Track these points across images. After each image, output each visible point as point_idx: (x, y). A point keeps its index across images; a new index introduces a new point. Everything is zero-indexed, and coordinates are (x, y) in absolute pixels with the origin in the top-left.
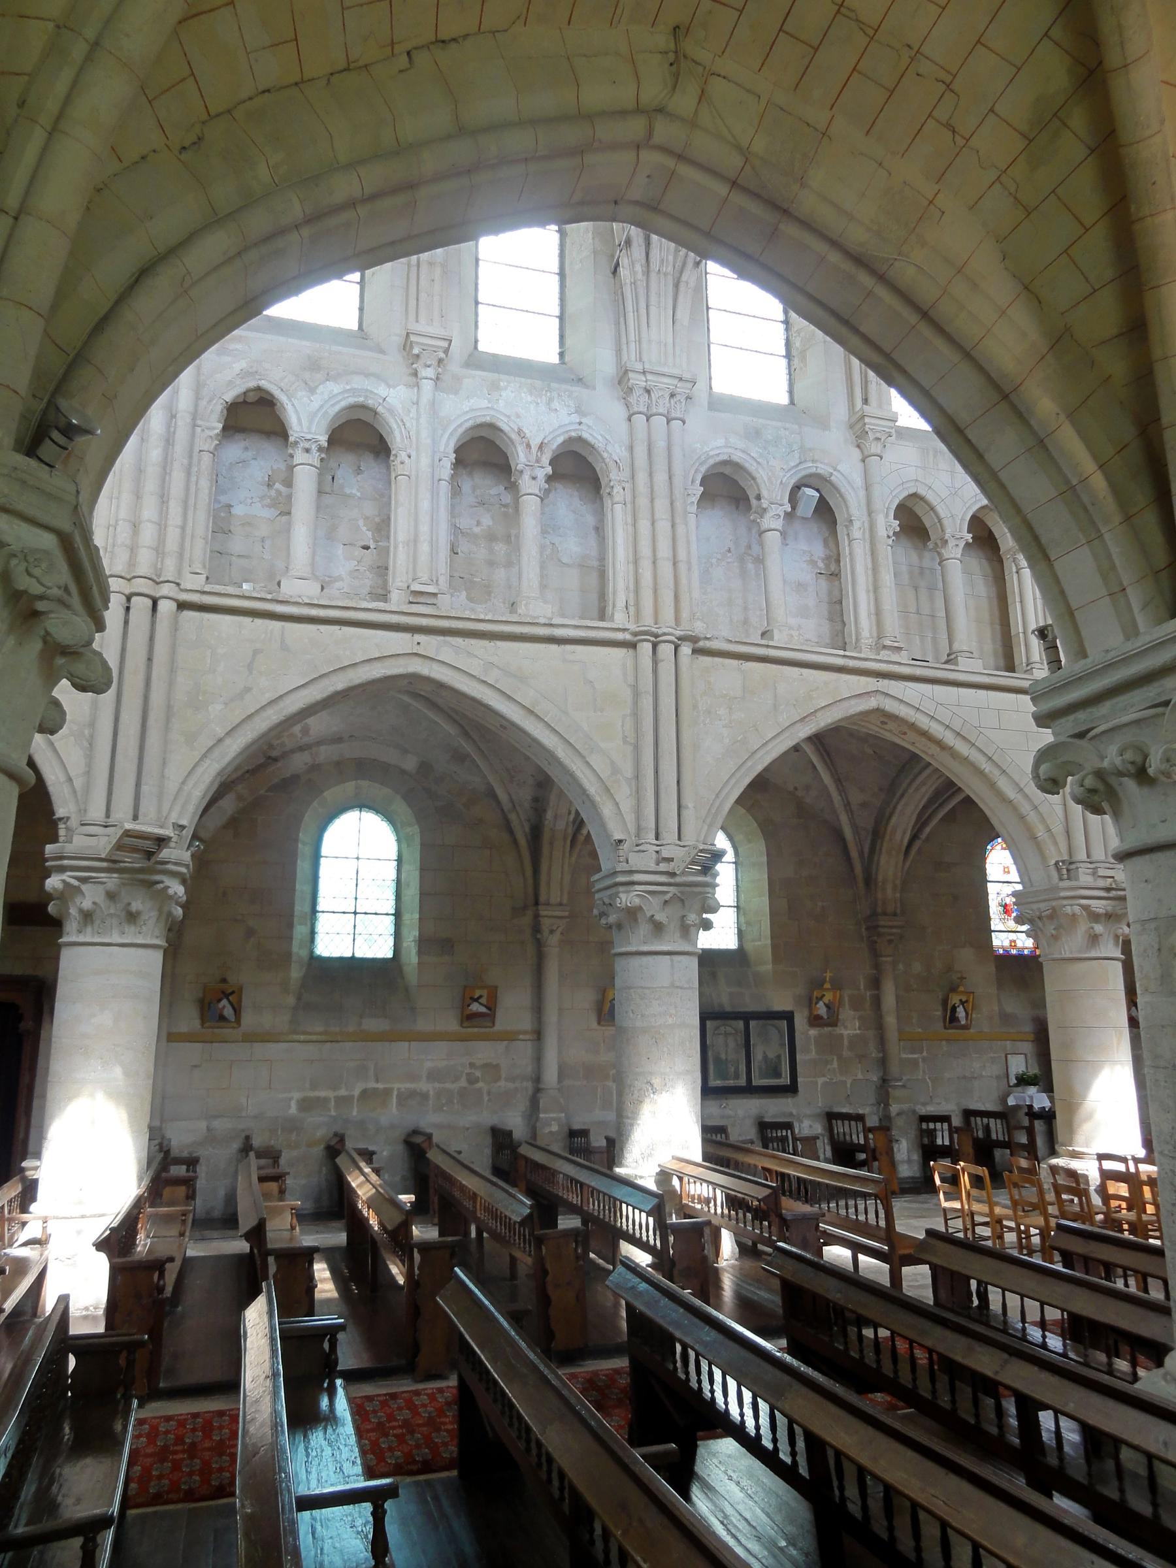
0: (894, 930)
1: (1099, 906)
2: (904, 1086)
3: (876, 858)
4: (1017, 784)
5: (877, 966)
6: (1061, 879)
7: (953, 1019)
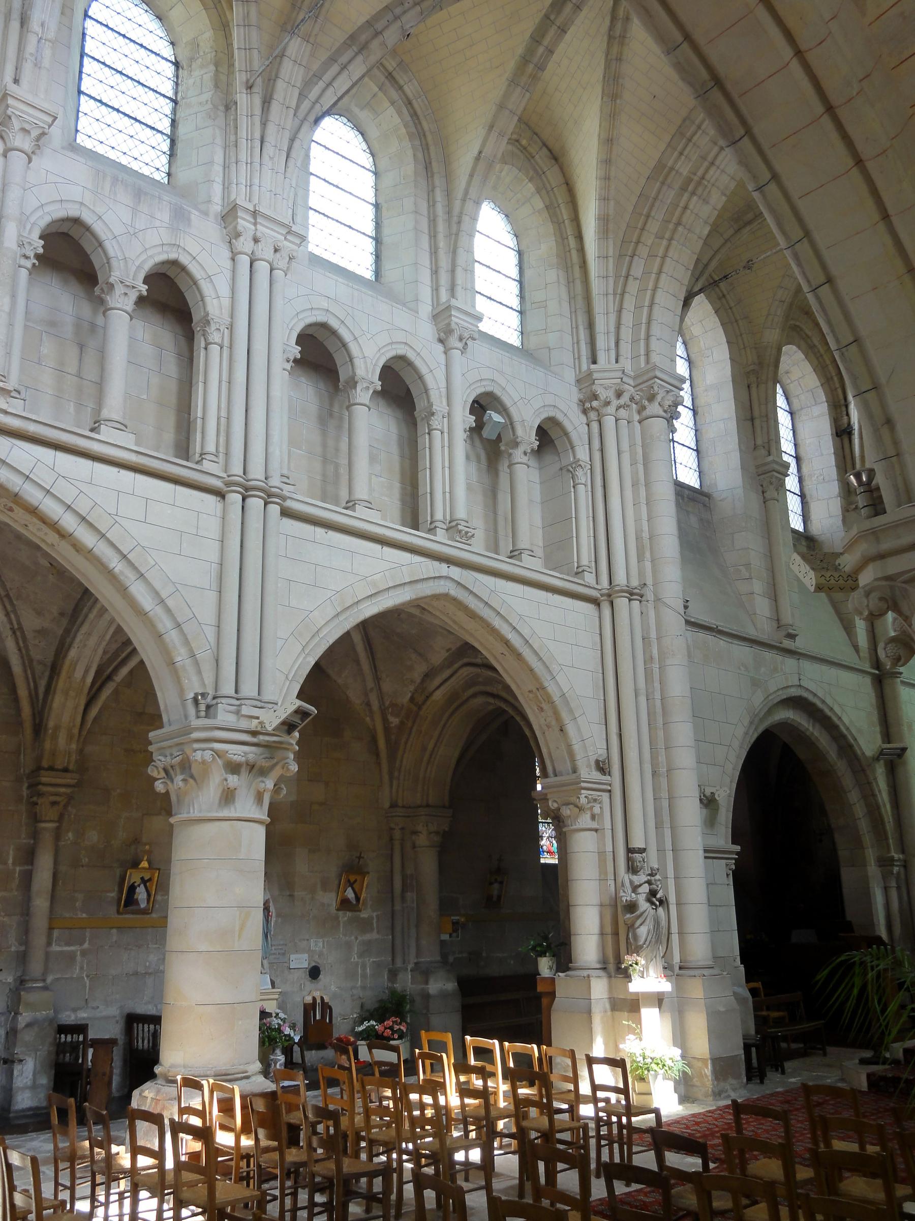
0: (62, 790)
1: (237, 753)
2: (46, 988)
3: (50, 698)
4: (157, 593)
5: (35, 835)
6: (198, 717)
7: (131, 900)
